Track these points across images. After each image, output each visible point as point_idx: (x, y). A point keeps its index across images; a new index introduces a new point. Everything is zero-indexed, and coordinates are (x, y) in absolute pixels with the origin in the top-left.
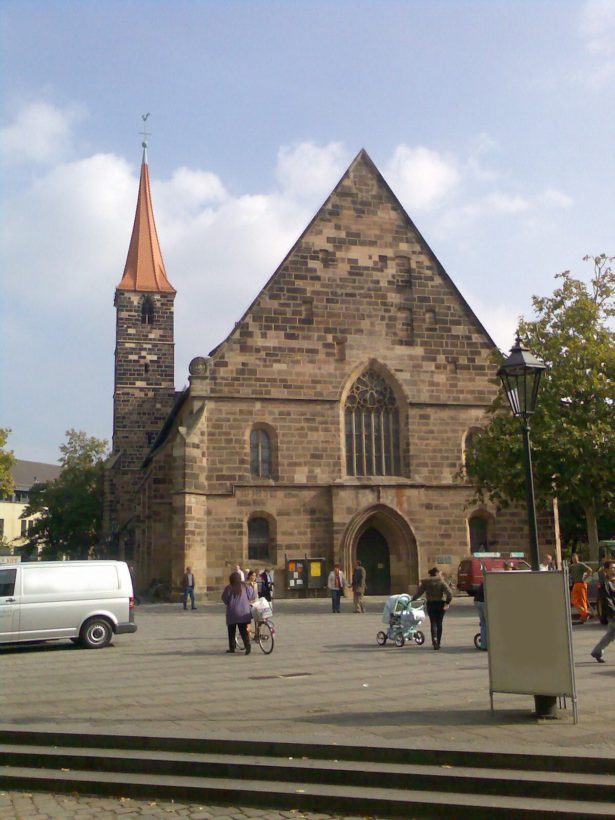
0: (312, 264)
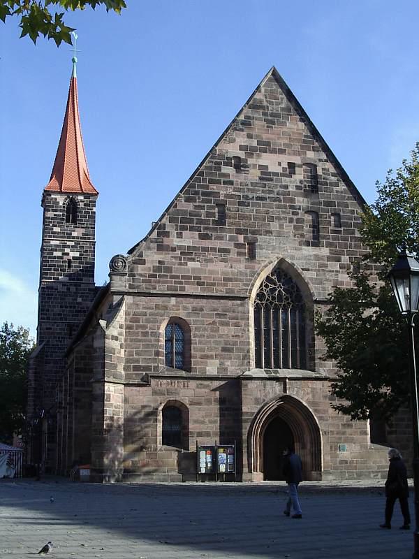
0: (225, 170)
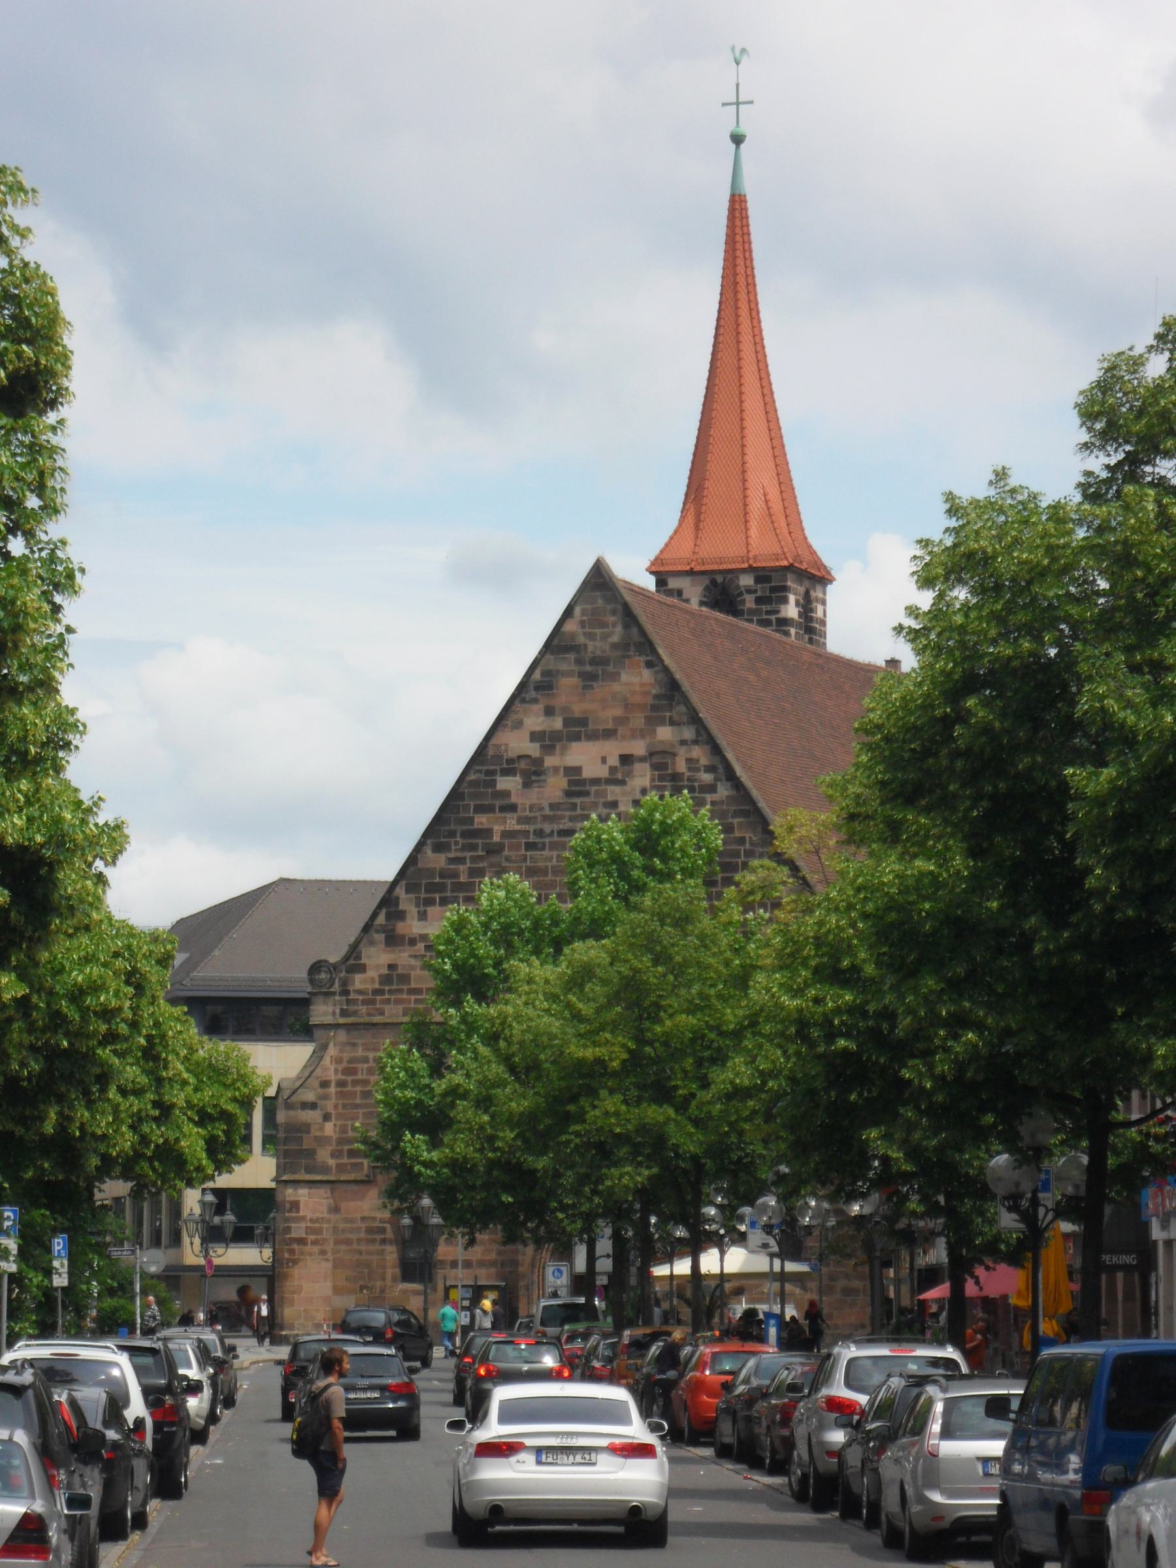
0: (505, 783)
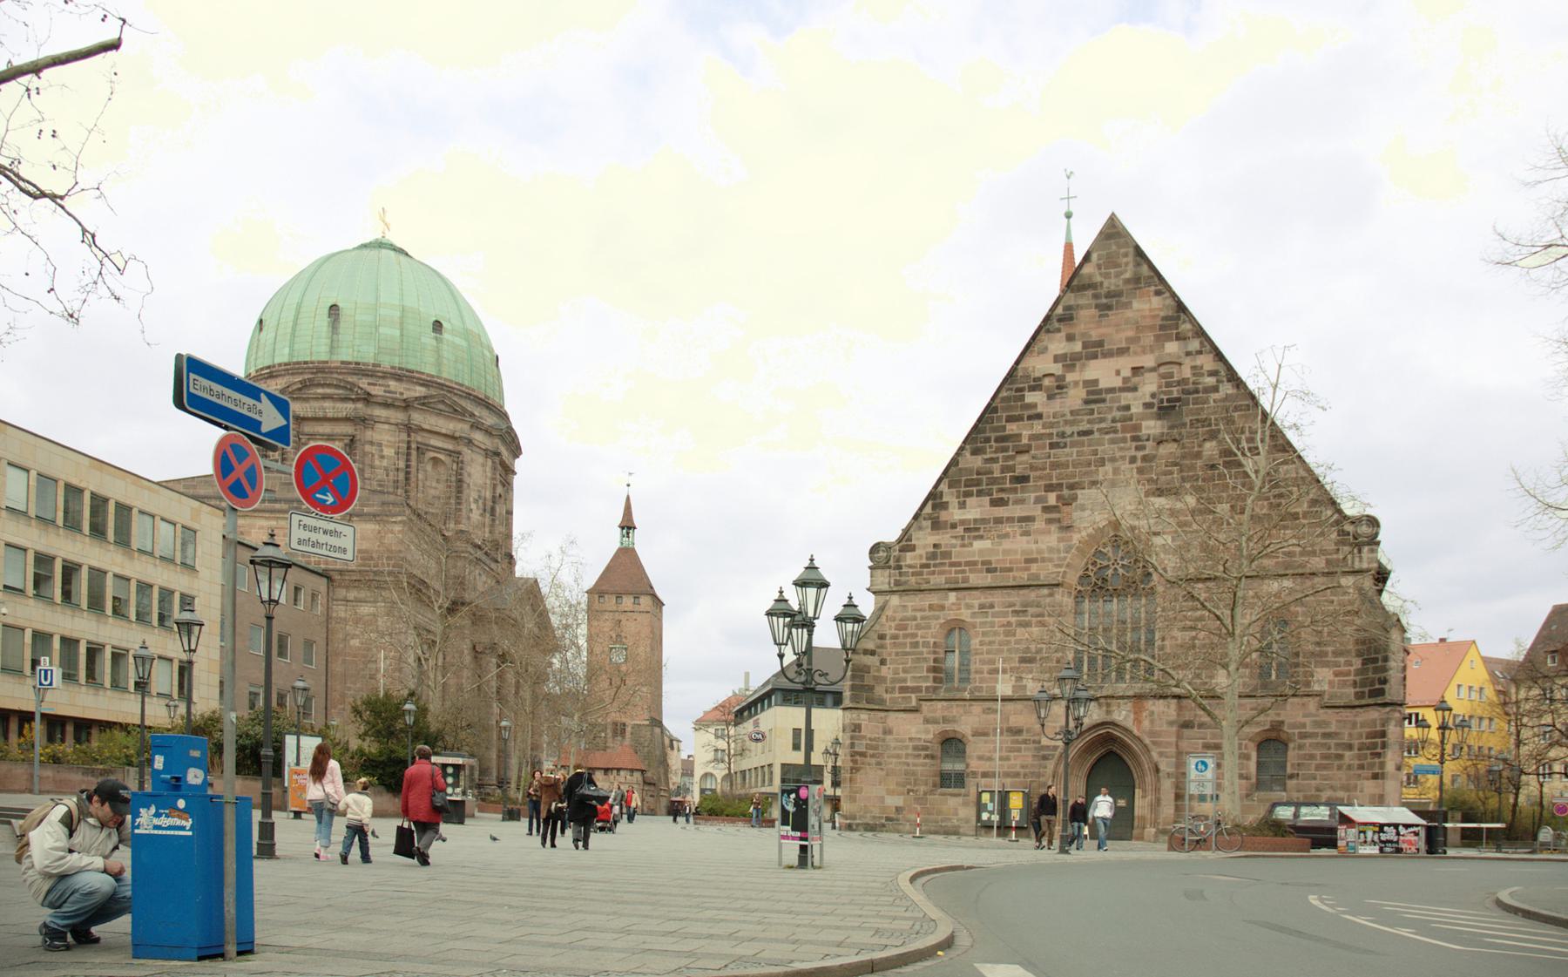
0: (1030, 397)
